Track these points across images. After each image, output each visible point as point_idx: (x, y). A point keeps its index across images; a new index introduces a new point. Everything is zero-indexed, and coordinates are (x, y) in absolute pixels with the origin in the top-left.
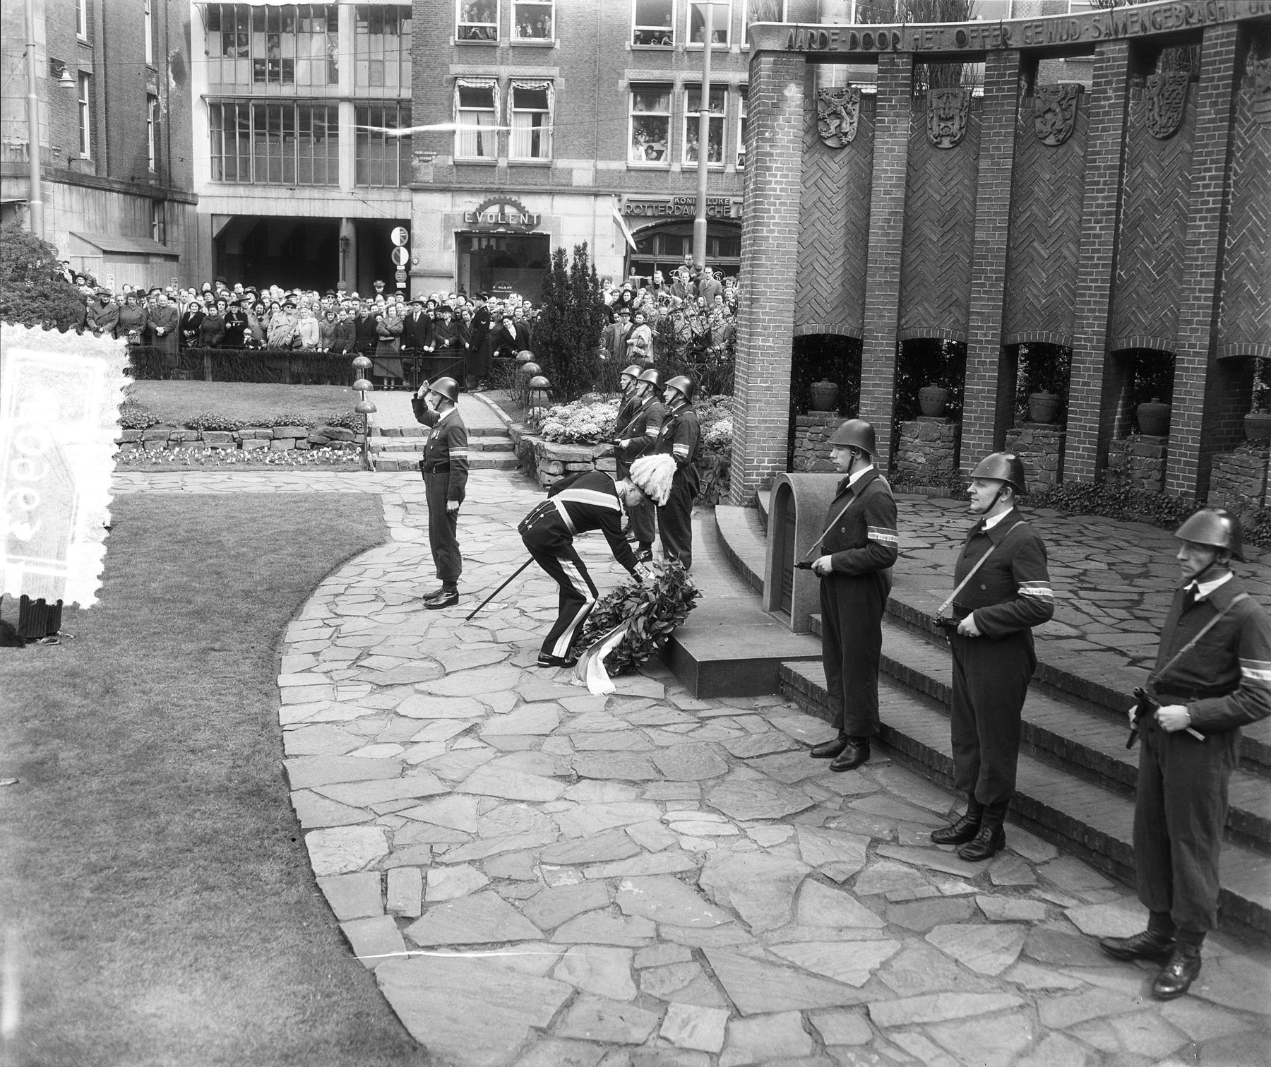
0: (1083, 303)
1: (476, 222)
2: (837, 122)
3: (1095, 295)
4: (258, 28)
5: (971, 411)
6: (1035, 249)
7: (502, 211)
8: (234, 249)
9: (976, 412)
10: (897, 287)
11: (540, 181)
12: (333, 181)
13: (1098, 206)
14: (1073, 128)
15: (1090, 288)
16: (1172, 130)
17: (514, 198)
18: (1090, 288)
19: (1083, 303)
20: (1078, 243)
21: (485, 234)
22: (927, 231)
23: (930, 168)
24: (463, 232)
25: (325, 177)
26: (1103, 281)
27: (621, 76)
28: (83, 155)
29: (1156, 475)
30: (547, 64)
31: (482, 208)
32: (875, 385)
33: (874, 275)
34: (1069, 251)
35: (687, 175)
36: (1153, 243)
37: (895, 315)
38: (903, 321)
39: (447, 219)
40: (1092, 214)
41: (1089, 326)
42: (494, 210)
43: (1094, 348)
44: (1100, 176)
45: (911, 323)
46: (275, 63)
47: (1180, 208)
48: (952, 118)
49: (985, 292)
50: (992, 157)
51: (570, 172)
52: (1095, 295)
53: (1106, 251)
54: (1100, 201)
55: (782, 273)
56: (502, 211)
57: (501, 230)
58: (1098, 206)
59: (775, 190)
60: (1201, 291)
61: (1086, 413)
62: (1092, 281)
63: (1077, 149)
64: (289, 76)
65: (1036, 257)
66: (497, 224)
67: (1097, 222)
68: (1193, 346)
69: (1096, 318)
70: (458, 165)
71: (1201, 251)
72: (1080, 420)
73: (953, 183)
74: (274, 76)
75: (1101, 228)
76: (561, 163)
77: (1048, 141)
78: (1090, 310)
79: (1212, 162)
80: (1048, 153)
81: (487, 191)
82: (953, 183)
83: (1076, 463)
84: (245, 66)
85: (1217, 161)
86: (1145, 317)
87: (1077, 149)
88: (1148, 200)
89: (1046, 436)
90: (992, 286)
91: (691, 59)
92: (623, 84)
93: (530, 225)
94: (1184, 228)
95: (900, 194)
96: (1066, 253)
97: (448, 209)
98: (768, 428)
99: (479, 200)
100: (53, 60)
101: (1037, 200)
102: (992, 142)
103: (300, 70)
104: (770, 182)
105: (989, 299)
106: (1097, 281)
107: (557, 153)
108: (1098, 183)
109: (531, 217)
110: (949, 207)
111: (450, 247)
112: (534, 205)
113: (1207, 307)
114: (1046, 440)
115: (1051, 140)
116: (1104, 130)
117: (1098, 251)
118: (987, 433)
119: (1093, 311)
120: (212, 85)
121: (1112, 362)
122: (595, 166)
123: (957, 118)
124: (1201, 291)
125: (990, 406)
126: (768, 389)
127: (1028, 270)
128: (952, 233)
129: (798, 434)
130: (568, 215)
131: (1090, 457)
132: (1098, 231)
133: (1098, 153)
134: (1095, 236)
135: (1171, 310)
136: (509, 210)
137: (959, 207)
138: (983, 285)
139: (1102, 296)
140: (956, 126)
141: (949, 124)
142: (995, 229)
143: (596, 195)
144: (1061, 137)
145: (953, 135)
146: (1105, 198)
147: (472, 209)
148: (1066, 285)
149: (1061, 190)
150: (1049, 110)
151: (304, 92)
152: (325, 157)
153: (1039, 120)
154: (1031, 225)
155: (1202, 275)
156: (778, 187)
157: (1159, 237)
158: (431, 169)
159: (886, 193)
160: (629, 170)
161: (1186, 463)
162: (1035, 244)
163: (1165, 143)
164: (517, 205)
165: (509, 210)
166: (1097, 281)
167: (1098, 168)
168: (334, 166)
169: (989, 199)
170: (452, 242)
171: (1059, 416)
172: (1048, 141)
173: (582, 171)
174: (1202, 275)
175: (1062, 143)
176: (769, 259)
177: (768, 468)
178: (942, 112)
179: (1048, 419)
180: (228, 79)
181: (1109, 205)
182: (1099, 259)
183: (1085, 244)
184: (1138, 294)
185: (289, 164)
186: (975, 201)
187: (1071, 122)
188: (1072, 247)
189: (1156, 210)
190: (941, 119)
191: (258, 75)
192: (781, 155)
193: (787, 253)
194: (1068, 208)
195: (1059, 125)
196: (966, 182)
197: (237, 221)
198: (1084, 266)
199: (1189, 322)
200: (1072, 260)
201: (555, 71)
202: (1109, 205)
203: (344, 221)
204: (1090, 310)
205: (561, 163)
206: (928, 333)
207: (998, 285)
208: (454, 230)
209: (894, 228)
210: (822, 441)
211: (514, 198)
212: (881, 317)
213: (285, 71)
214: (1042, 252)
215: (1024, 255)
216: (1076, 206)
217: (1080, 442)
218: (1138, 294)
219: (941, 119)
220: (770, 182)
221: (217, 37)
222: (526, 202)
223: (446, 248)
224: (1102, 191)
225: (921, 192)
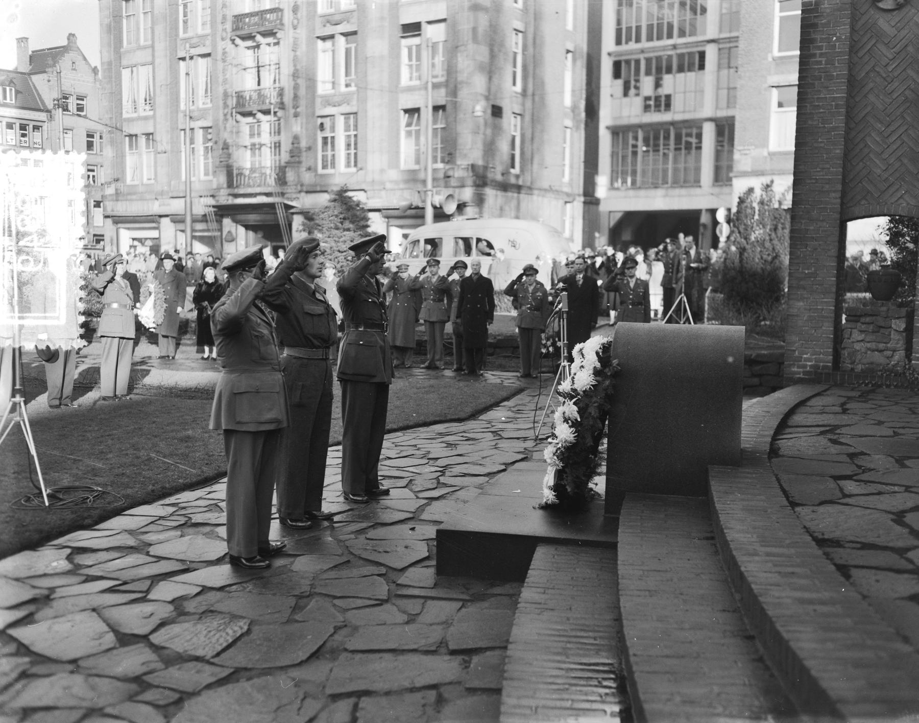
4: (648, 73)
8: (627, 236)
12: (697, 183)
25: (691, 180)
28: (512, 171)
46: (657, 99)
64: (668, 106)
70: (772, 155)
74: (658, 106)
84: (638, 102)
100: (494, 107)
103: (677, 103)
104: (814, 55)
120: (615, 118)
151: (679, 117)
152: (691, 164)
156: (823, 60)
168: (698, 170)
177: (809, 360)
180: (625, 113)
185: (665, 171)
191: (647, 108)
193: (834, 129)
197: (629, 217)
203: (704, 213)
213: (664, 103)
221: (620, 82)
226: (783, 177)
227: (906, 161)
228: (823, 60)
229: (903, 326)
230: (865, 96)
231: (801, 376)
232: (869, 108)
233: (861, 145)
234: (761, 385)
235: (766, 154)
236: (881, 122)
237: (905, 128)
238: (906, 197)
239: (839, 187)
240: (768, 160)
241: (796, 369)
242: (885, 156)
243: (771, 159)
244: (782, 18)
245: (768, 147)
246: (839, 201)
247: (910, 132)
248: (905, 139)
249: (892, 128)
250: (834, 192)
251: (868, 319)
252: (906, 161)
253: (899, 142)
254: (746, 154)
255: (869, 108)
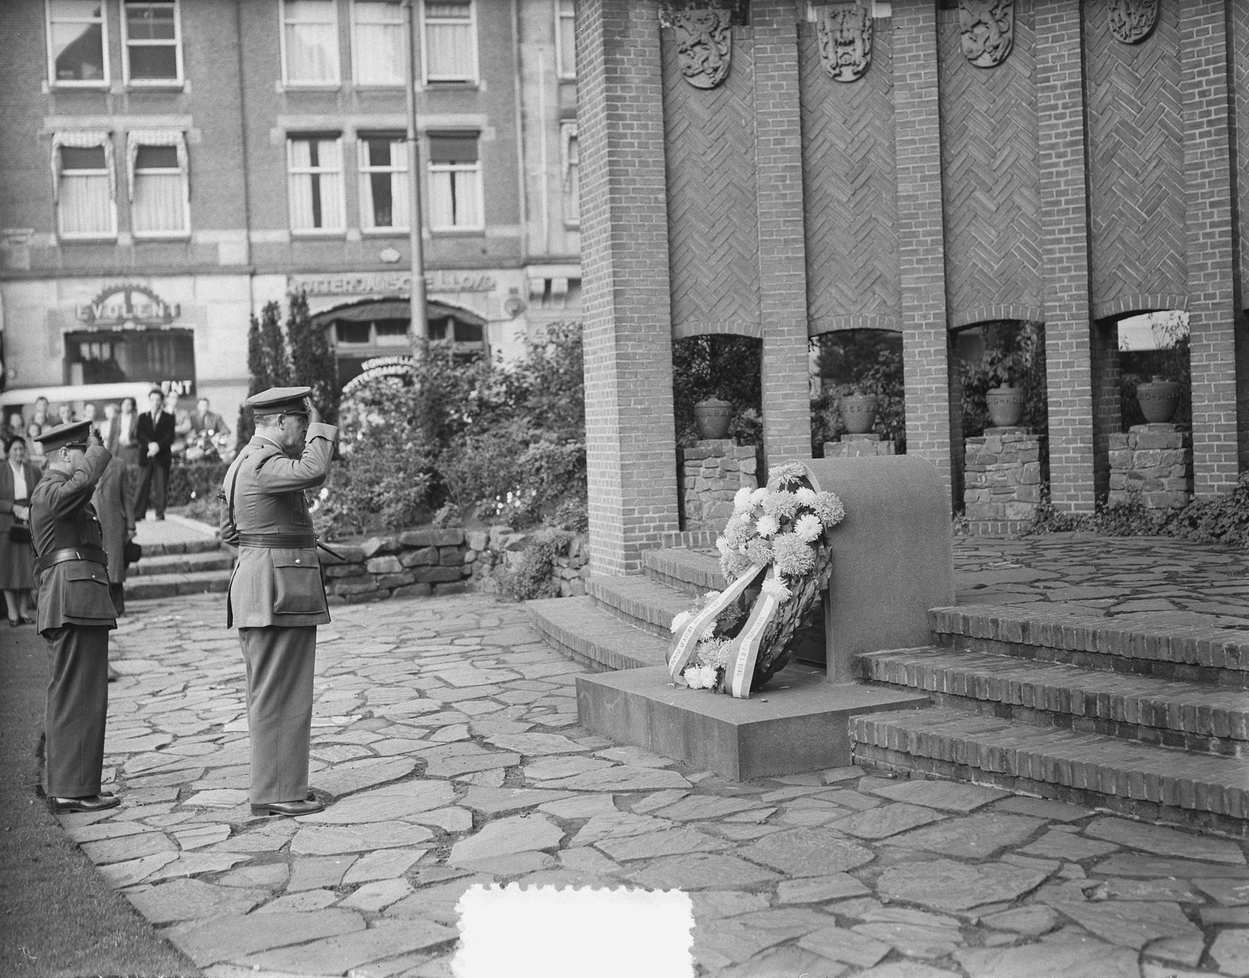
0: (1051, 261)
1: (92, 318)
2: (705, 53)
3: (1068, 250)
5: (917, 419)
6: (978, 201)
7: (128, 300)
9: (922, 418)
10: (803, 263)
11: (177, 258)
13: (1058, 136)
14: (1011, 44)
15: (1059, 241)
16: (1146, 30)
17: (142, 282)
18: (1059, 241)
19: (1051, 261)
20: (1037, 188)
21: (105, 336)
22: (831, 190)
23: (828, 108)
24: (75, 333)
26: (1077, 230)
27: (273, 125)
29: (1179, 470)
30: (176, 112)
31: (101, 299)
32: (786, 396)
33: (769, 251)
34: (1025, 200)
35: (368, 243)
36: (1137, 175)
37: (803, 300)
38: (813, 309)
39: (53, 317)
40: (1052, 147)
41: (1064, 289)
42: (117, 300)
43: (1073, 317)
44: (1057, 97)
45: (822, 312)
47: (1167, 127)
48: (852, 42)
49: (919, 261)
50: (911, 88)
51: (215, 247)
52: (1068, 250)
53: (1075, 192)
54: (1061, 130)
55: (651, 255)
56: (128, 300)
57: (129, 326)
58: (1058, 136)
59: (632, 145)
60: (1213, 225)
61: (1072, 403)
62: (1061, 231)
63: (1020, 68)
65: (980, 211)
66: (121, 320)
67: (1059, 156)
68: (1213, 296)
69: (1071, 279)
70: (65, 245)
71: (1205, 175)
72: (1066, 413)
73: (861, 126)
75: (1066, 164)
76: (202, 237)
77: (980, 62)
78: (1062, 270)
79: (1208, 62)
80: (982, 76)
81: (109, 274)
82: (861, 126)
83: (1066, 469)
85: (1215, 61)
86: (1137, 270)
87: (1020, 68)
88: (1123, 123)
89: (1020, 441)
90: (927, 252)
91: (361, 100)
92: (277, 134)
93: (168, 318)
94: (1179, 153)
95: (794, 142)
96: (1019, 200)
97: (53, 303)
98: (651, 466)
99: (95, 287)
101: (974, 138)
102: (909, 68)
105: (925, 270)
106: (1068, 230)
107: (197, 223)
108: (1055, 107)
109: (166, 308)
110: (858, 156)
111: (59, 352)
112: (172, 290)
113: (1224, 244)
114: (1019, 446)
115: (986, 60)
116: (1055, 39)
117: (1065, 193)
118: (941, 445)
119: (1069, 269)
121: (1097, 334)
122: (248, 238)
123: (858, 43)
124: (1213, 225)
125: (941, 409)
126: (646, 411)
127: (972, 228)
128: (866, 189)
129: (688, 471)
130: (217, 302)
131: (1084, 460)
132: (1062, 169)
133: (1052, 69)
134: (1059, 174)
135: (1172, 257)
136: (138, 299)
137: (871, 156)
138: (915, 252)
139: (1077, 249)
140: (859, 52)
141: (849, 49)
142: (923, 179)
143: (253, 274)
144: (998, 55)
145: (855, 64)
146: (1066, 125)
147: (87, 301)
148: (1025, 243)
149: (1004, 123)
150: (979, 23)
153: (967, 35)
154: (968, 171)
155: (1212, 205)
157: (1144, 167)
158: (27, 253)
159: (777, 142)
160: (294, 239)
161: (1220, 448)
162: (978, 194)
163: (1137, 49)
164: (147, 292)
165: (138, 299)
166: (1068, 230)
167: (1054, 88)
169: (913, 142)
170: (61, 345)
171: (1033, 417)
172: (980, 62)
173: (231, 246)
174: (1212, 205)
175: (1001, 62)
176: (631, 236)
178: (838, 35)
179: (1015, 420)
181: (1073, 133)
182: (1067, 202)
183: (1046, 186)
184: (1124, 243)
186: (892, 146)
187: (1010, 34)
188: (1026, 192)
189: (1136, 133)
190: (838, 44)
192: (636, 99)
194: (1016, 144)
195: (994, 40)
196: (877, 123)
198: (1048, 213)
199: (1202, 267)
200: (1029, 210)
201: (187, 121)
202: (1073, 133)
204: (1062, 270)
205: (202, 237)
206: (847, 321)
207: (935, 250)
208: (63, 330)
209: (792, 187)
210: (722, 477)
211: (142, 282)
212: (785, 305)
214: (986, 202)
215: (964, 209)
216: (1027, 140)
217: (1068, 441)
218: (1124, 243)
219: (838, 44)
220: (625, 136)
222: (160, 286)
223: (53, 354)
224: (1062, 116)
225: (820, 139)
226: (87, 280)
227: (736, 270)
228: (636, 142)
229: (754, 467)
230: (682, 189)
231: (644, 542)
232: (688, 205)
233: (684, 249)
234: (416, 582)
235: (53, 241)
236: (703, 221)
237: (733, 229)
238: (742, 312)
239: (668, 300)
240: (59, 252)
241: (637, 533)
242: (712, 262)
243: (63, 252)
244: (172, 36)
245: (56, 230)
246: (668, 317)
247: (738, 235)
248: (734, 244)
249: (718, 228)
250: (663, 305)
251: (710, 461)
252: (736, 270)
253: (726, 247)
254: (18, 243)
255: (688, 205)
